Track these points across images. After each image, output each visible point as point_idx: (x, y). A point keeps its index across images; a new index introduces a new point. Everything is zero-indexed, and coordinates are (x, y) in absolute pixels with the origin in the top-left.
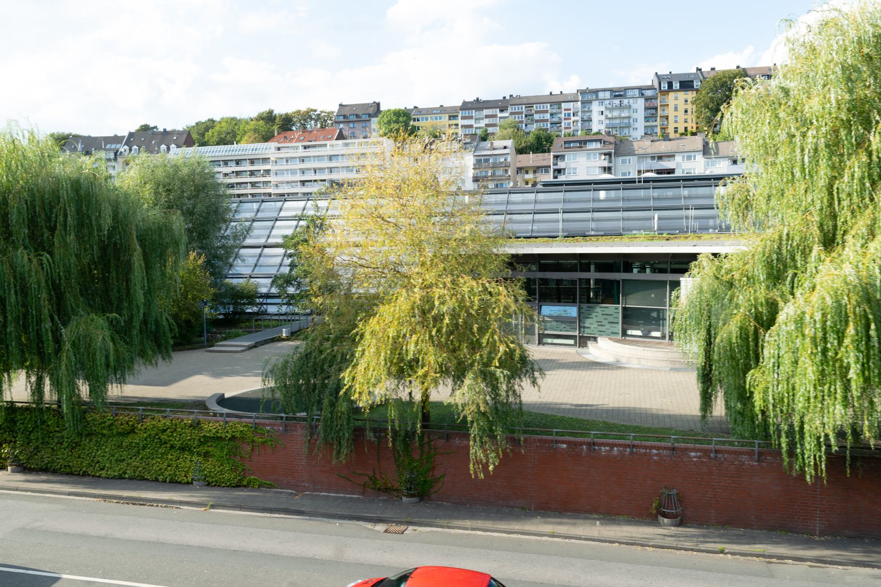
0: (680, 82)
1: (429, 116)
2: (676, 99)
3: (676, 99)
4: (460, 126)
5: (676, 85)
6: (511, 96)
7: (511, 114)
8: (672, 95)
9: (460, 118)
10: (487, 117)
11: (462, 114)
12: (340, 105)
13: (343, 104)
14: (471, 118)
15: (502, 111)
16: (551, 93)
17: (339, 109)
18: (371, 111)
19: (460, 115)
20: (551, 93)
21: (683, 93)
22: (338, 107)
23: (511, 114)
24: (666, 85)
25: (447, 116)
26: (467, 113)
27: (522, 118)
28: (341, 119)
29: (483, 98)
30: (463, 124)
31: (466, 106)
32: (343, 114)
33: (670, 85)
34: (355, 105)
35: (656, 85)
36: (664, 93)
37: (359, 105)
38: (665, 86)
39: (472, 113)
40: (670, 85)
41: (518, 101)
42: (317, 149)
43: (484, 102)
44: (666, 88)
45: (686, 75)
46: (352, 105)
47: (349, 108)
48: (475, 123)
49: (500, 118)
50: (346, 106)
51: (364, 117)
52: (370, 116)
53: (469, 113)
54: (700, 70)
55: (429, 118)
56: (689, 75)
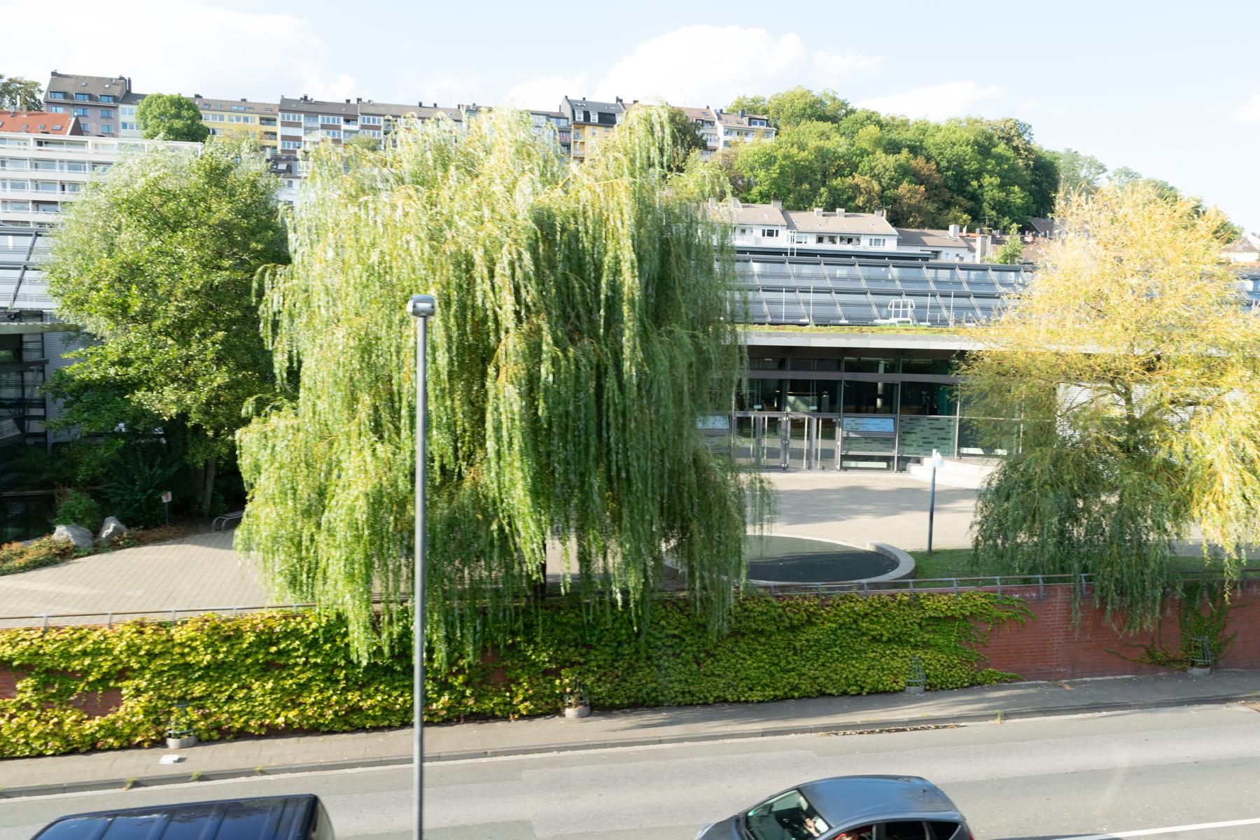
0: (600, 114)
1: (226, 115)
2: (594, 134)
3: (594, 134)
4: (279, 137)
5: (594, 118)
6: (359, 100)
7: (363, 127)
8: (588, 129)
9: (279, 123)
10: (323, 127)
11: (283, 118)
12: (54, 74)
13: (59, 72)
14: (298, 125)
15: (347, 121)
16: (420, 105)
17: (52, 81)
18: (117, 91)
19: (279, 120)
20: (420, 105)
21: (603, 129)
22: (49, 77)
23: (363, 127)
24: (582, 116)
25: (257, 117)
26: (291, 117)
27: (379, 134)
28: (59, 98)
29: (317, 95)
30: (285, 134)
31: (287, 106)
32: (62, 89)
33: (587, 116)
34: (85, 77)
35: (568, 114)
36: (579, 126)
37: (92, 78)
38: (580, 117)
39: (299, 119)
40: (587, 116)
41: (372, 110)
42: (65, 148)
43: (317, 103)
44: (582, 120)
45: (605, 105)
46: (77, 77)
47: (72, 81)
48: (305, 134)
49: (345, 131)
50: (66, 76)
51: (104, 102)
52: (115, 99)
53: (294, 118)
54: (621, 101)
55: (226, 118)
56: (609, 105)
